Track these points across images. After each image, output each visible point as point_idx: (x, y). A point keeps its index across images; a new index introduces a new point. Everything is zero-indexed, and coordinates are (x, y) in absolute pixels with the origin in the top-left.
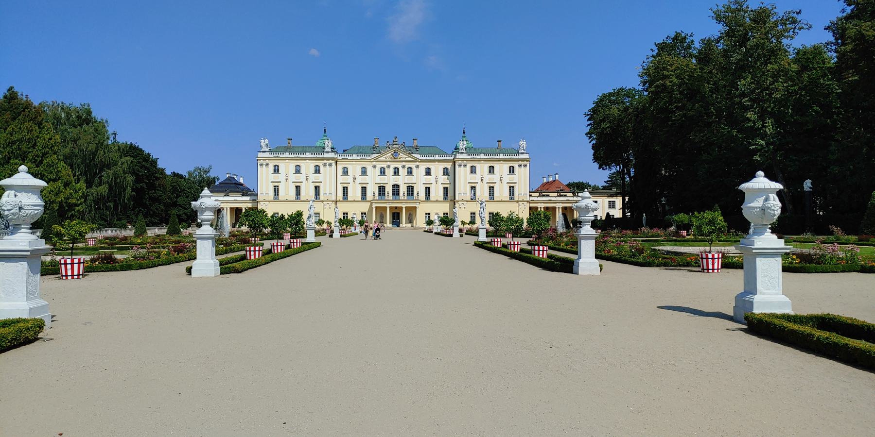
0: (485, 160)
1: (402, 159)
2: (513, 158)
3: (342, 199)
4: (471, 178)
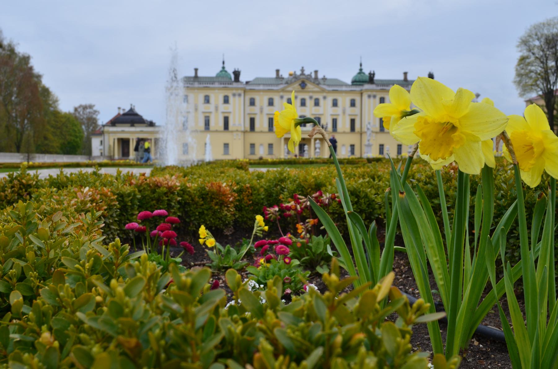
1: (309, 90)
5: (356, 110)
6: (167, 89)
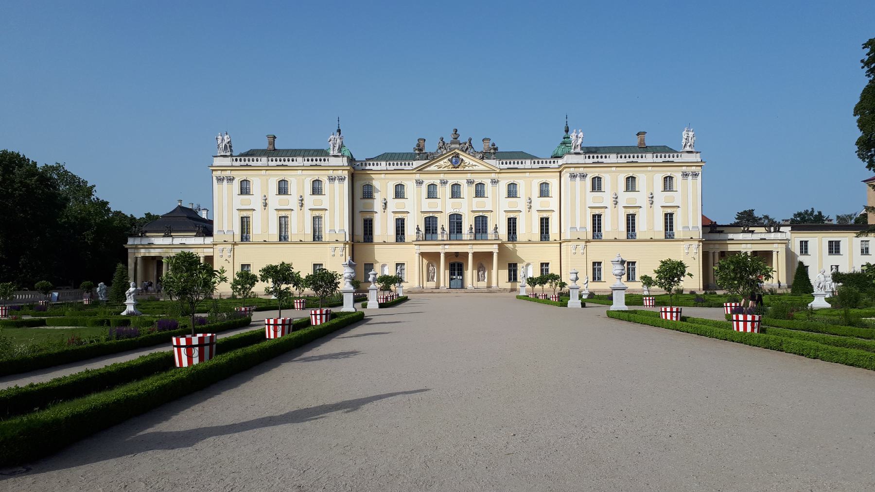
0: (618, 166)
1: (467, 168)
2: (672, 162)
3: (362, 240)
4: (592, 198)
5: (552, 202)
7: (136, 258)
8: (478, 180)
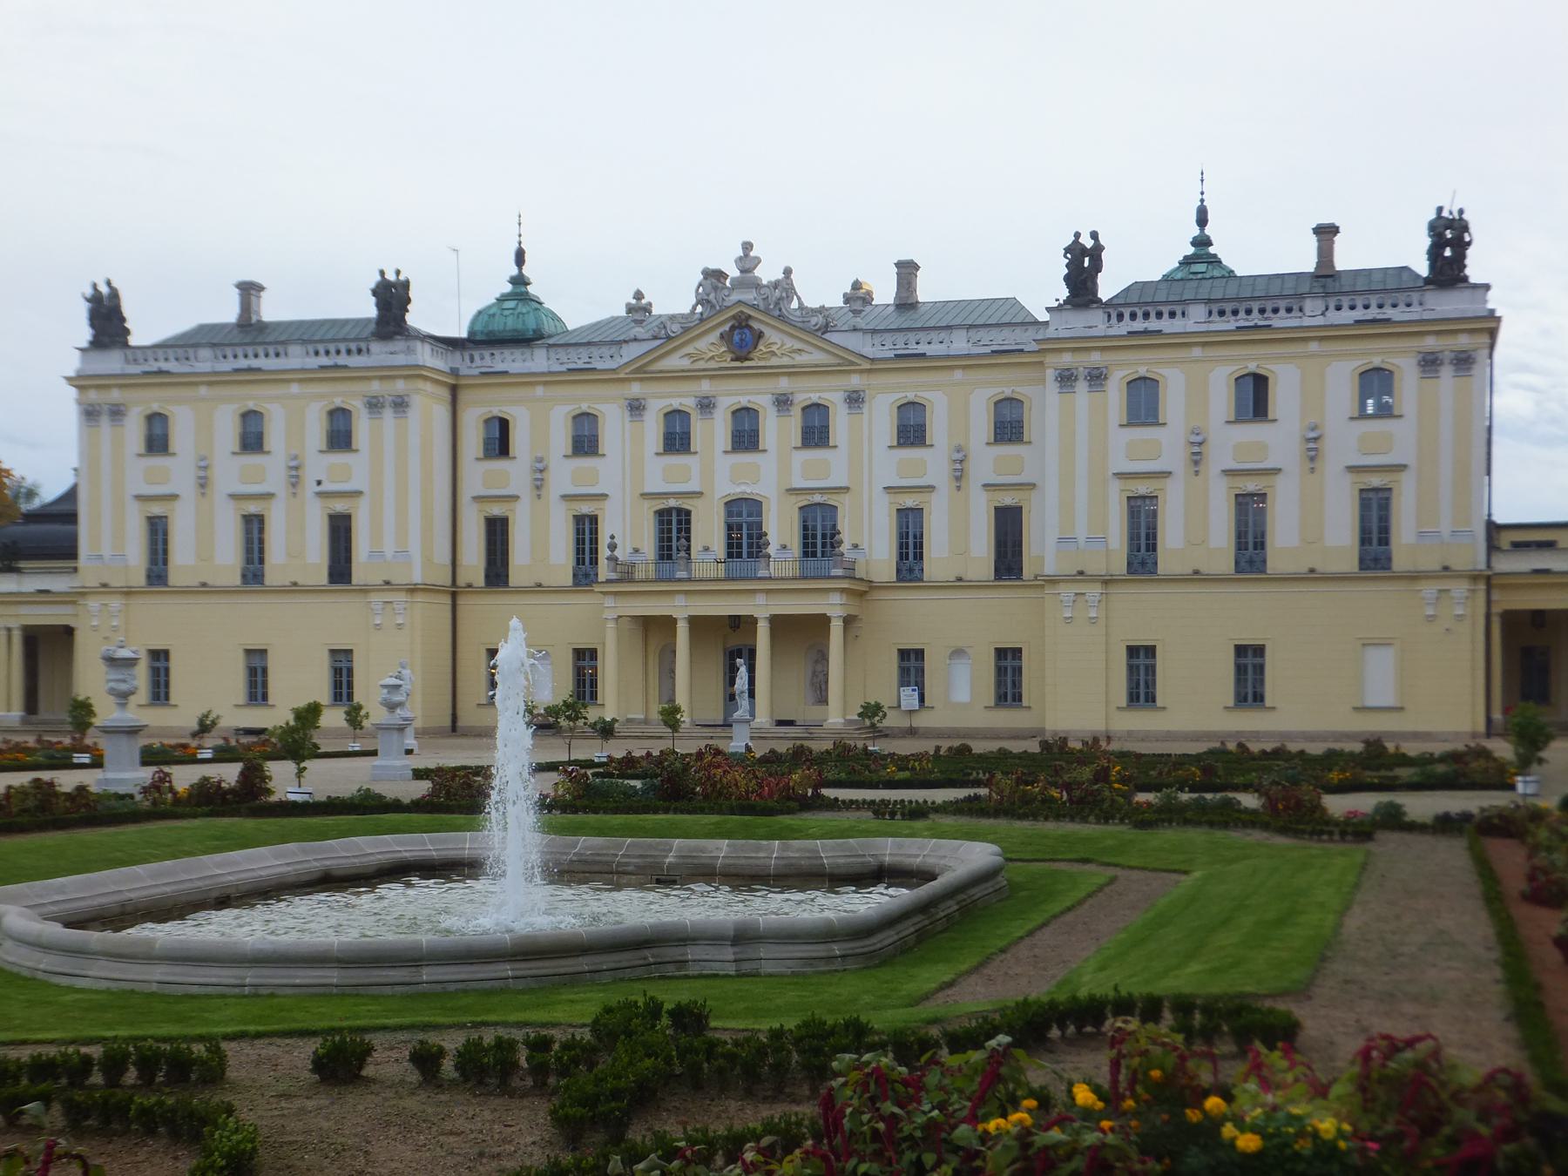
1: (774, 361)
3: (479, 579)
6: (80, 382)
7: (9, 630)
8: (806, 396)
